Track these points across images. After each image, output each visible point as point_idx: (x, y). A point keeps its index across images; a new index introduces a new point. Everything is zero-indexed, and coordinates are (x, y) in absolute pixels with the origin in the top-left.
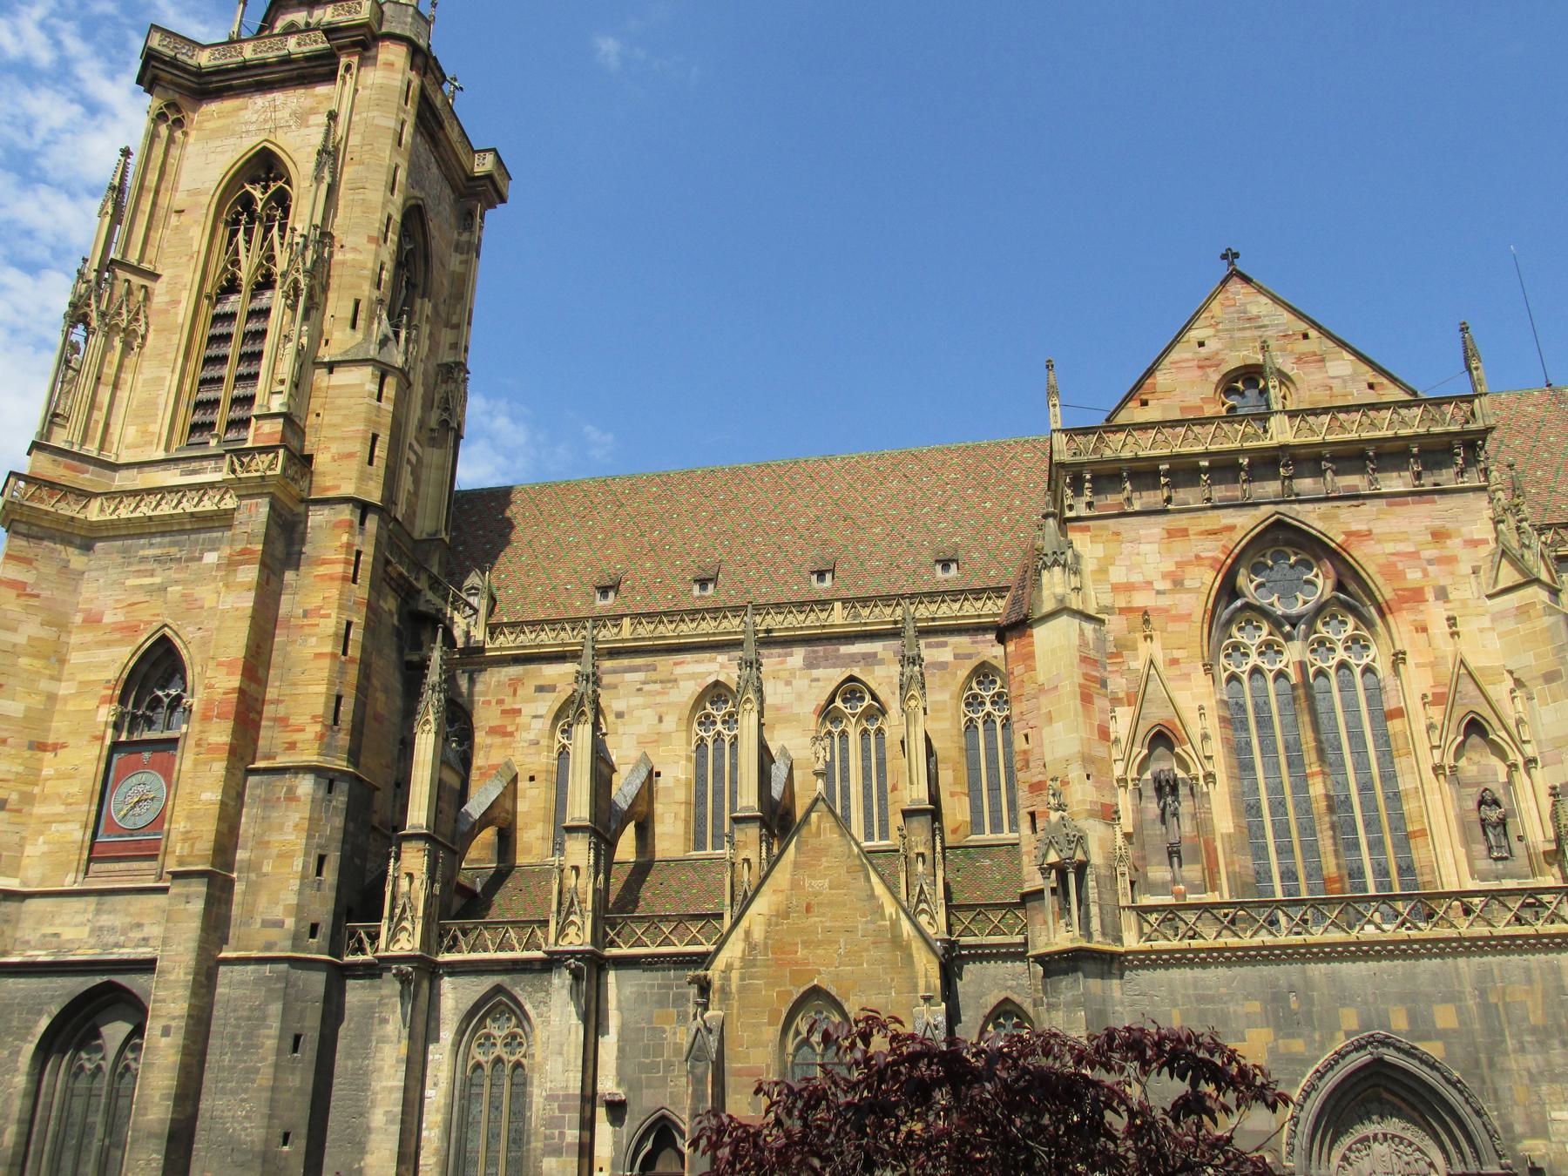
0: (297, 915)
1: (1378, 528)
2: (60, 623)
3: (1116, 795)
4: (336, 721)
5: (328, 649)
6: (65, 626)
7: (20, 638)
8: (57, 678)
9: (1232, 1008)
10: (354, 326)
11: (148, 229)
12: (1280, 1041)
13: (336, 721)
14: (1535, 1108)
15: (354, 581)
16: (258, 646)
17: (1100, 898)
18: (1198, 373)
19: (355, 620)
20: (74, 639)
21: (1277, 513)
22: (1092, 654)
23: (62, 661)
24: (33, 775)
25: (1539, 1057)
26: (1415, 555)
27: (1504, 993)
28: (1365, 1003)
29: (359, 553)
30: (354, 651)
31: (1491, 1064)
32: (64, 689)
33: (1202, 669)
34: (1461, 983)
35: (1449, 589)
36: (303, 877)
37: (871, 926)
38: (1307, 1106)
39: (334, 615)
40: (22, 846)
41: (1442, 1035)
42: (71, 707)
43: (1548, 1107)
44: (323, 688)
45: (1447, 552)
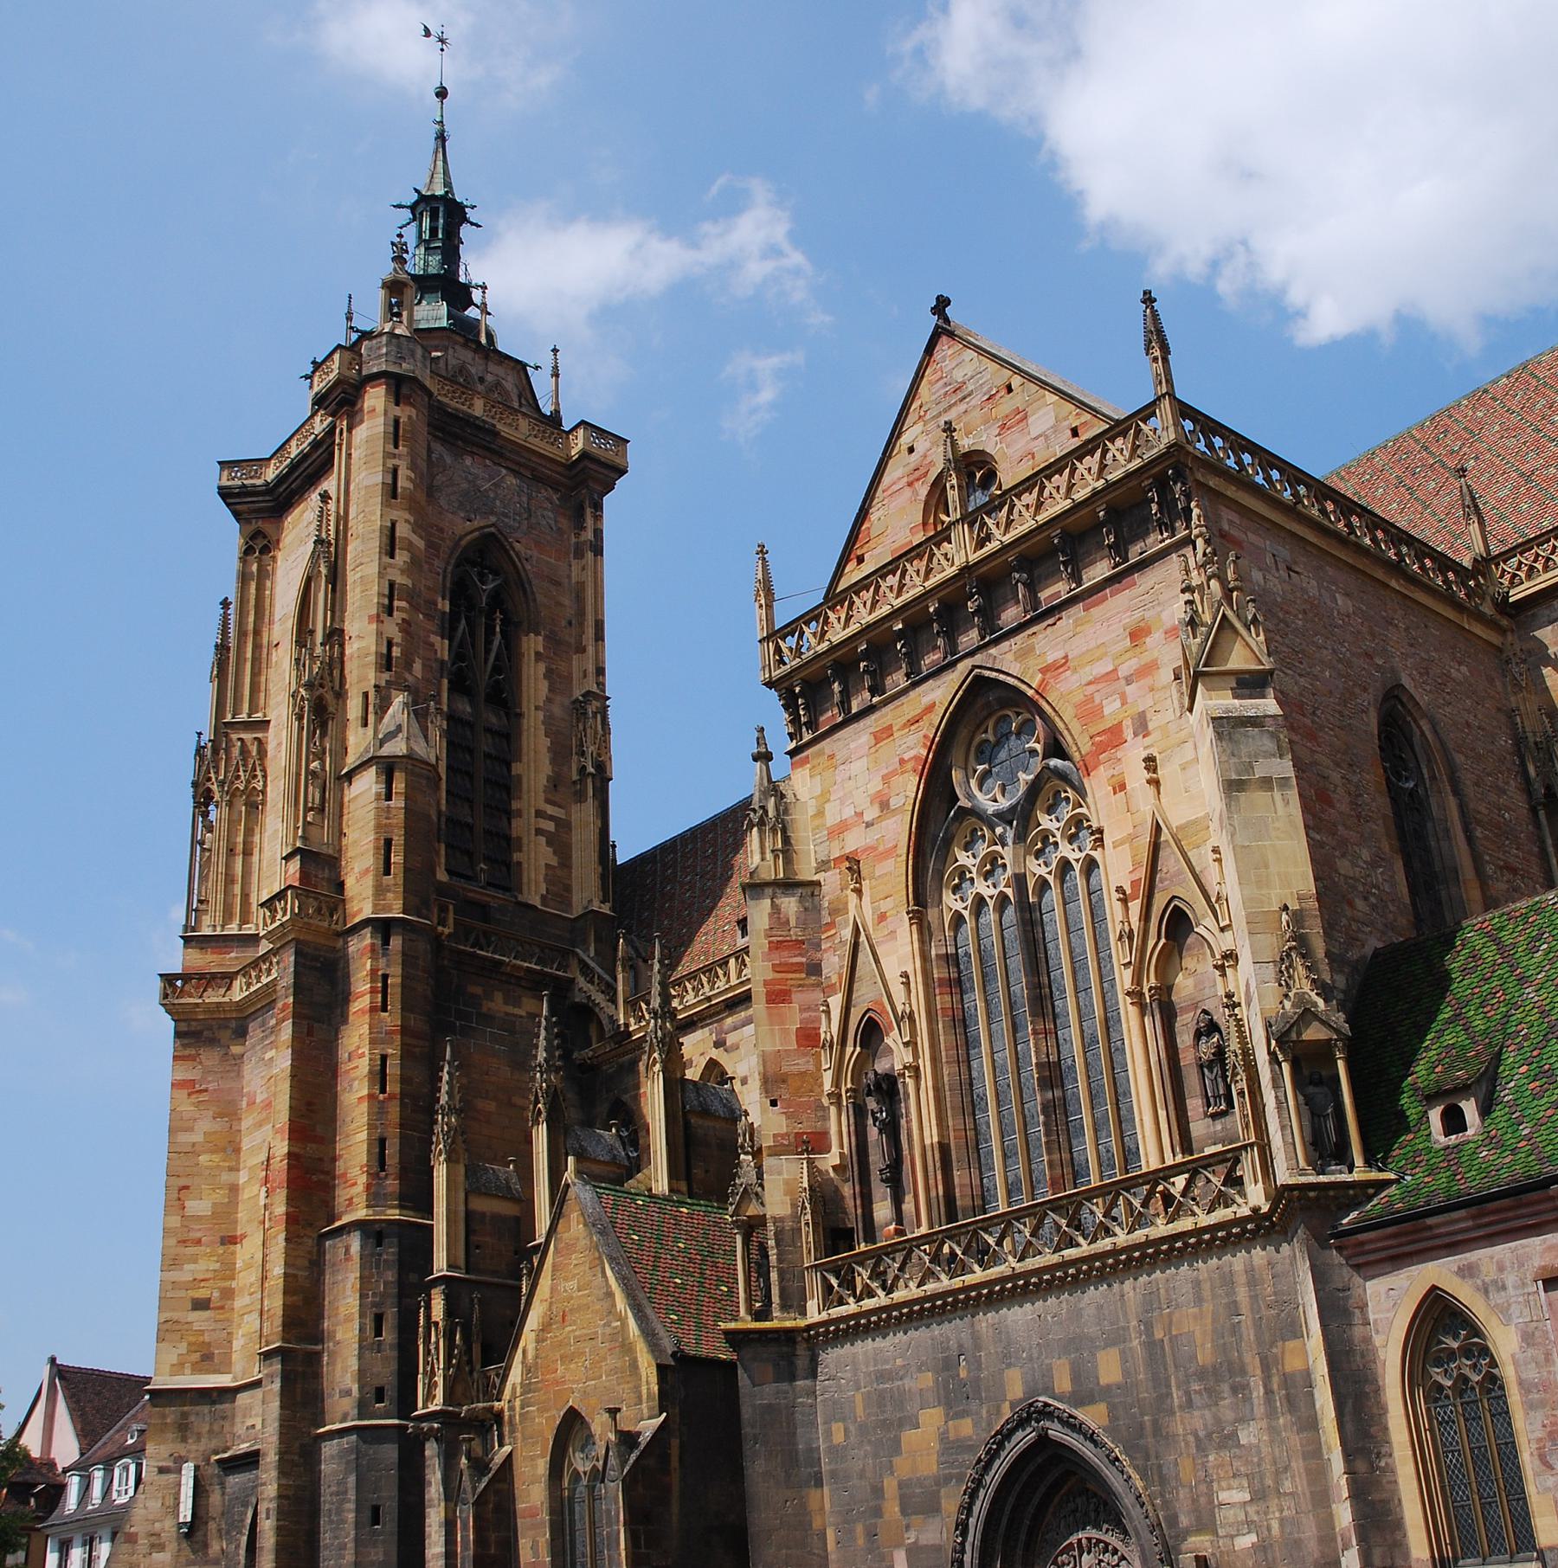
0: (359, 1381)
1: (1076, 648)
2: (229, 1111)
3: (826, 1118)
4: (382, 1165)
5: (365, 1092)
6: (236, 1114)
7: (197, 1137)
8: (235, 1169)
9: (908, 1383)
10: (365, 724)
11: (256, 674)
12: (950, 1423)
13: (383, 1169)
14: (1203, 1488)
15: (384, 1009)
16: (309, 1104)
17: (780, 1260)
18: (908, 492)
19: (390, 1051)
20: (246, 1124)
21: (975, 667)
22: (795, 934)
23: (237, 1150)
24: (228, 1271)
25: (1207, 1412)
26: (1111, 676)
27: (1171, 1323)
28: (1030, 1359)
29: (385, 977)
30: (393, 1087)
31: (1157, 1429)
32: (243, 1177)
33: (906, 918)
34: (1125, 1314)
35: (1148, 716)
36: (361, 1341)
37: (608, 1330)
38: (976, 1509)
39: (367, 1052)
40: (230, 1342)
41: (1106, 1393)
42: (246, 1197)
43: (1215, 1485)
44: (364, 1135)
45: (1146, 658)
